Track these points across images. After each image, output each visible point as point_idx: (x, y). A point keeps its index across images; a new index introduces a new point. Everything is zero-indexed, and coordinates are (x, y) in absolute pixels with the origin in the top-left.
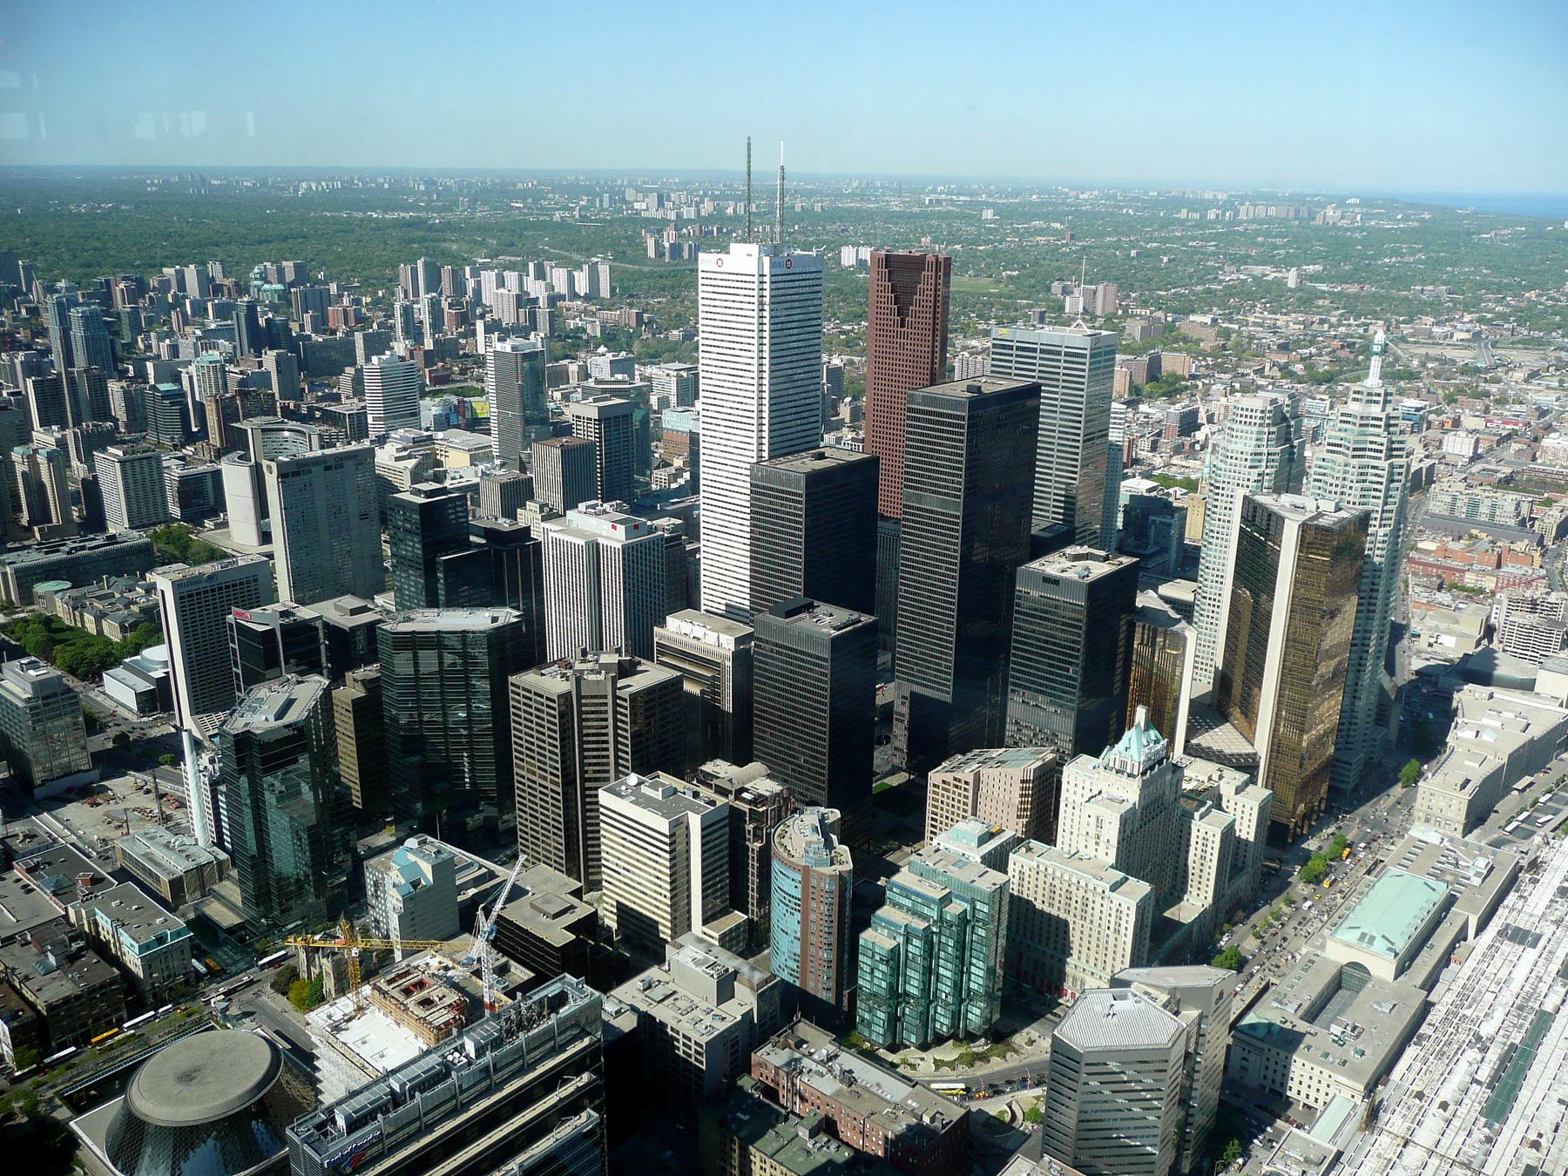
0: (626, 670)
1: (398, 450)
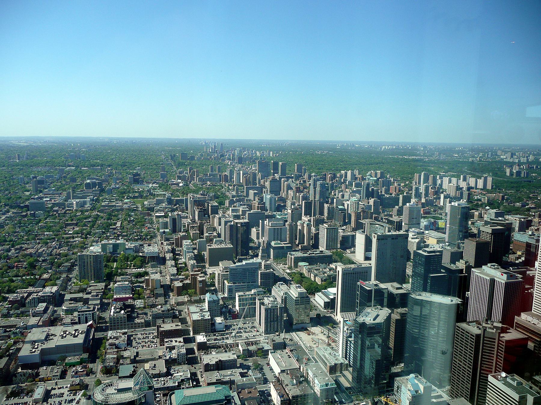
0: (504, 330)
1: (413, 235)
